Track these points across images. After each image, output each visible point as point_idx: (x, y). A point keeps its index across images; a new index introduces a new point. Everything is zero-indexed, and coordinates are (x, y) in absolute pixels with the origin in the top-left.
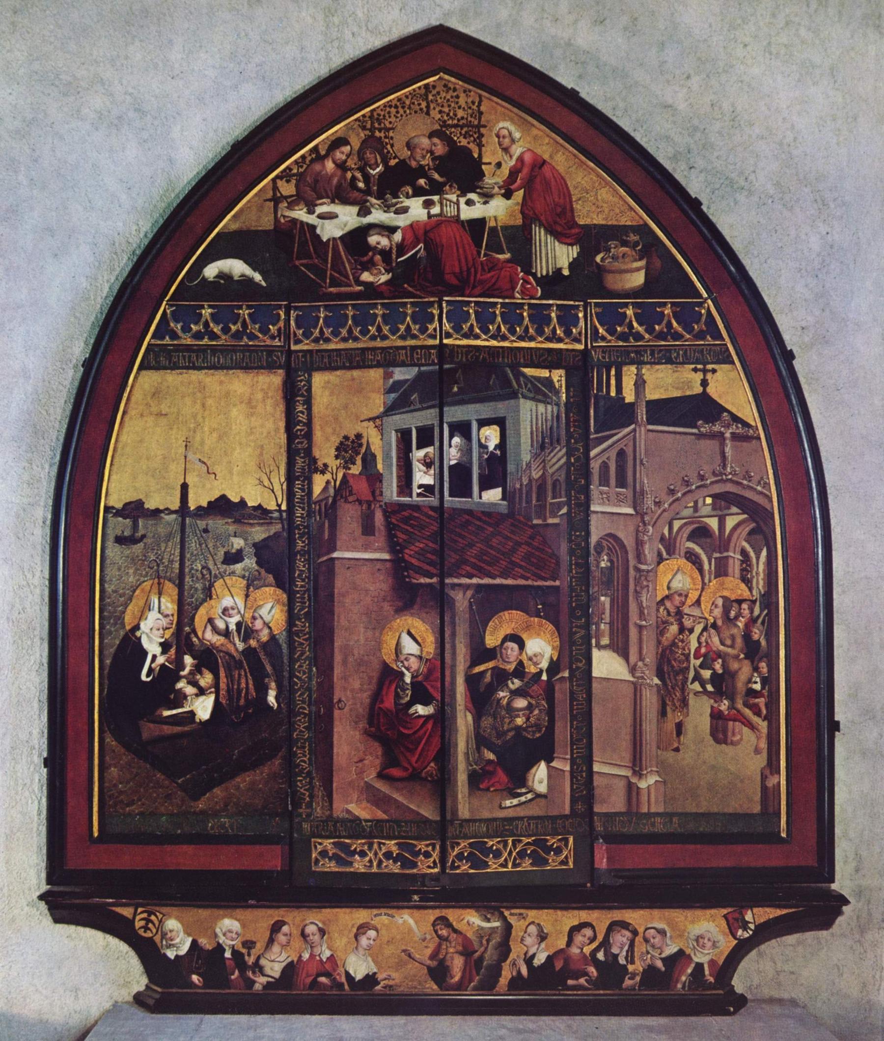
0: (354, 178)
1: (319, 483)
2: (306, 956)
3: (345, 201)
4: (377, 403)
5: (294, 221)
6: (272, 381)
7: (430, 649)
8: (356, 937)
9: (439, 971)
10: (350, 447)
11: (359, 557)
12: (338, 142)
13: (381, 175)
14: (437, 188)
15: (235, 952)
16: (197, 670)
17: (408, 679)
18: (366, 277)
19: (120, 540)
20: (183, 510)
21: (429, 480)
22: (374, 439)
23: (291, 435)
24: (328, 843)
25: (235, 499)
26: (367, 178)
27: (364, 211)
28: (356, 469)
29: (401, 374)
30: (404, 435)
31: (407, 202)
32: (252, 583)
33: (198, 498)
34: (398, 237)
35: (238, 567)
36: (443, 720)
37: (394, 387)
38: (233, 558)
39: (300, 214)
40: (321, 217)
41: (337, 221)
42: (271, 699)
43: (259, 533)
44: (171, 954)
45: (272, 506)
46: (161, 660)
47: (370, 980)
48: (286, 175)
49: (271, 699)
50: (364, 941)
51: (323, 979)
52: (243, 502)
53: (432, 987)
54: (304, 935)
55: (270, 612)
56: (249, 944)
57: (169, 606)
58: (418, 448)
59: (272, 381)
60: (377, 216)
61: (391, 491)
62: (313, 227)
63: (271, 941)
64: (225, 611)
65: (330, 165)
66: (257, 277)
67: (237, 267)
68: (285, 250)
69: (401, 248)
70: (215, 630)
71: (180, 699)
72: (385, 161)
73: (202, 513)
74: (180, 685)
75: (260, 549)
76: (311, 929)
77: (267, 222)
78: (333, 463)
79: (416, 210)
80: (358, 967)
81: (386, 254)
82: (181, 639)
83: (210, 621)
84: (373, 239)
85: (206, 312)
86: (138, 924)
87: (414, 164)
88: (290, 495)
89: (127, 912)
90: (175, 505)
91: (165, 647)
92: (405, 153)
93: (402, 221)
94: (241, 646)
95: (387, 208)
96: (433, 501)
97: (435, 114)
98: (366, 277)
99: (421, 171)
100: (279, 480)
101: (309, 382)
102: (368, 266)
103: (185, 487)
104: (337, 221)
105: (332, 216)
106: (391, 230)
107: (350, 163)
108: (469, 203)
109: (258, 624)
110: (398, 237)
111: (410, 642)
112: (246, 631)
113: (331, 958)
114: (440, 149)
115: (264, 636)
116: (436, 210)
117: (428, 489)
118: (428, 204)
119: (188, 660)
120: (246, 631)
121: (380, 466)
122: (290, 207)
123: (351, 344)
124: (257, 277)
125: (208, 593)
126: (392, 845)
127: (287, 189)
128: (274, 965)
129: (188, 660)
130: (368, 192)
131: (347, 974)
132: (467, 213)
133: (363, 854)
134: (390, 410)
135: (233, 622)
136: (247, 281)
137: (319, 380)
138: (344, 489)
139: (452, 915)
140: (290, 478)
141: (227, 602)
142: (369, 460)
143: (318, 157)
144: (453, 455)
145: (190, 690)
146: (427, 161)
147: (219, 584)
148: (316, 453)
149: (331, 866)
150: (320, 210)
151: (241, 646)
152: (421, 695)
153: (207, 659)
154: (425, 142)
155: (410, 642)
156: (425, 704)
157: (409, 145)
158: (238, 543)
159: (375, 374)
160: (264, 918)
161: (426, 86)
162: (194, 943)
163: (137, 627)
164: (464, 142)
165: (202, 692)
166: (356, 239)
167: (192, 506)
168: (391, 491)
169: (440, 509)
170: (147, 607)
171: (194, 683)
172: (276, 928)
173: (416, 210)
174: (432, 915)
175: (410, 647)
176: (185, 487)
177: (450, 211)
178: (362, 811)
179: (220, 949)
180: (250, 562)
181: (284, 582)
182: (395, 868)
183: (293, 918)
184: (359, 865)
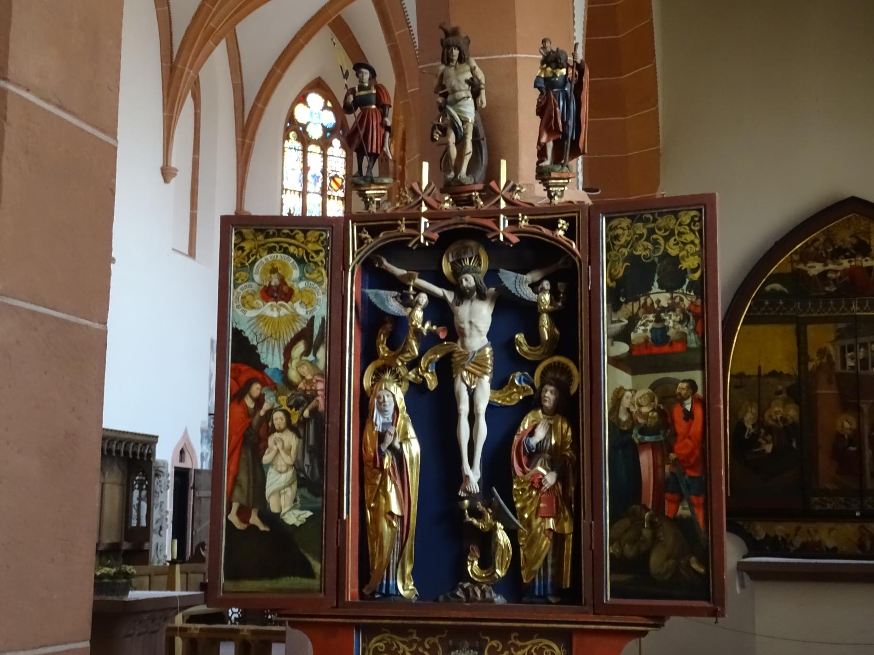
0: (821, 254)
1: (810, 365)
2: (810, 540)
3: (819, 261)
4: (832, 337)
5: (799, 269)
6: (791, 328)
7: (855, 426)
8: (829, 533)
9: (861, 546)
10: (822, 352)
11: (826, 391)
12: (815, 240)
13: (832, 252)
14: (853, 256)
15: (783, 539)
16: (766, 434)
17: (846, 436)
18: (827, 289)
19: (737, 387)
20: (759, 375)
21: (852, 364)
22: (831, 349)
23: (799, 348)
24: (817, 499)
25: (778, 370)
26: (826, 253)
27: (826, 265)
28: (825, 360)
29: (841, 325)
30: (843, 349)
31: (842, 261)
32: (785, 402)
33: (765, 371)
34: (839, 274)
35: (780, 396)
36: (860, 453)
37: (839, 330)
38: (780, 393)
39: (801, 266)
40: (810, 267)
41: (815, 269)
42: (794, 445)
43: (788, 384)
44: (758, 538)
45: (792, 373)
46: (752, 430)
47: (835, 549)
48: (796, 252)
49: (794, 445)
50: (832, 534)
51: (817, 549)
52: (781, 373)
53: (859, 552)
54: (808, 532)
55: (792, 412)
56: (788, 535)
57: (755, 410)
58: (849, 351)
59: (791, 328)
60: (831, 266)
61: (838, 368)
62: (806, 272)
63: (796, 534)
64: (776, 413)
65: (812, 249)
66: (786, 290)
67: (777, 286)
68: (796, 279)
69: (840, 278)
70: (773, 420)
71: (759, 445)
72: (833, 247)
73: (766, 376)
74: (760, 440)
75: (789, 390)
76: (811, 530)
77: (788, 269)
78: (816, 358)
79: (846, 264)
80: (830, 544)
81: (834, 280)
82: (759, 423)
83: (770, 416)
84: (830, 275)
85: (767, 303)
86: (746, 527)
87: (844, 247)
88: (799, 370)
89: (741, 523)
90: (756, 373)
91: (754, 425)
92: (841, 244)
93: (840, 268)
94: (782, 425)
95: (834, 263)
96: (853, 371)
97: (852, 229)
98: (827, 289)
99: (847, 250)
100: (795, 365)
101: (806, 328)
102: (828, 285)
103: (760, 368)
104: (815, 269)
105: (814, 267)
106: (836, 271)
107: (821, 247)
108: (866, 261)
109: (788, 418)
110: (839, 274)
111: (847, 424)
112: (784, 419)
113: (820, 541)
114: (854, 241)
115: (791, 421)
116: (853, 264)
117: (852, 367)
118: (850, 262)
119: (762, 431)
120: (784, 419)
121: (834, 359)
122: (798, 264)
123: (821, 315)
124: (786, 290)
125: (769, 406)
126: (842, 499)
127: (796, 258)
128: (798, 542)
129: (762, 431)
130: (827, 258)
131: (826, 547)
132: (866, 264)
133: (830, 503)
134: (837, 338)
135: (779, 416)
136: (781, 292)
137: (810, 328)
138: (819, 368)
139: (866, 525)
140: (799, 363)
141: (777, 409)
142: (829, 357)
143: (807, 245)
144: (861, 354)
145: (763, 442)
146: (849, 246)
147: (773, 403)
148: (809, 354)
149: (818, 508)
150: (809, 265)
151: (782, 425)
152: (851, 442)
153: (769, 430)
154: (848, 239)
155: (847, 424)
156: (853, 446)
157: (843, 241)
158: (780, 387)
159: (831, 326)
160: (793, 525)
161: (848, 219)
162: (767, 535)
163: (743, 419)
164: (863, 238)
165: (768, 442)
166: (823, 275)
167: (763, 373)
168: (838, 368)
169: (857, 375)
170: (746, 412)
171: (765, 439)
172: (798, 529)
173: (846, 264)
174: (857, 525)
175: (847, 425)
176: (760, 368)
177: (859, 263)
178: (830, 486)
179: (776, 537)
180: (784, 395)
181: (797, 402)
182: (844, 508)
183: (804, 526)
184: (829, 507)
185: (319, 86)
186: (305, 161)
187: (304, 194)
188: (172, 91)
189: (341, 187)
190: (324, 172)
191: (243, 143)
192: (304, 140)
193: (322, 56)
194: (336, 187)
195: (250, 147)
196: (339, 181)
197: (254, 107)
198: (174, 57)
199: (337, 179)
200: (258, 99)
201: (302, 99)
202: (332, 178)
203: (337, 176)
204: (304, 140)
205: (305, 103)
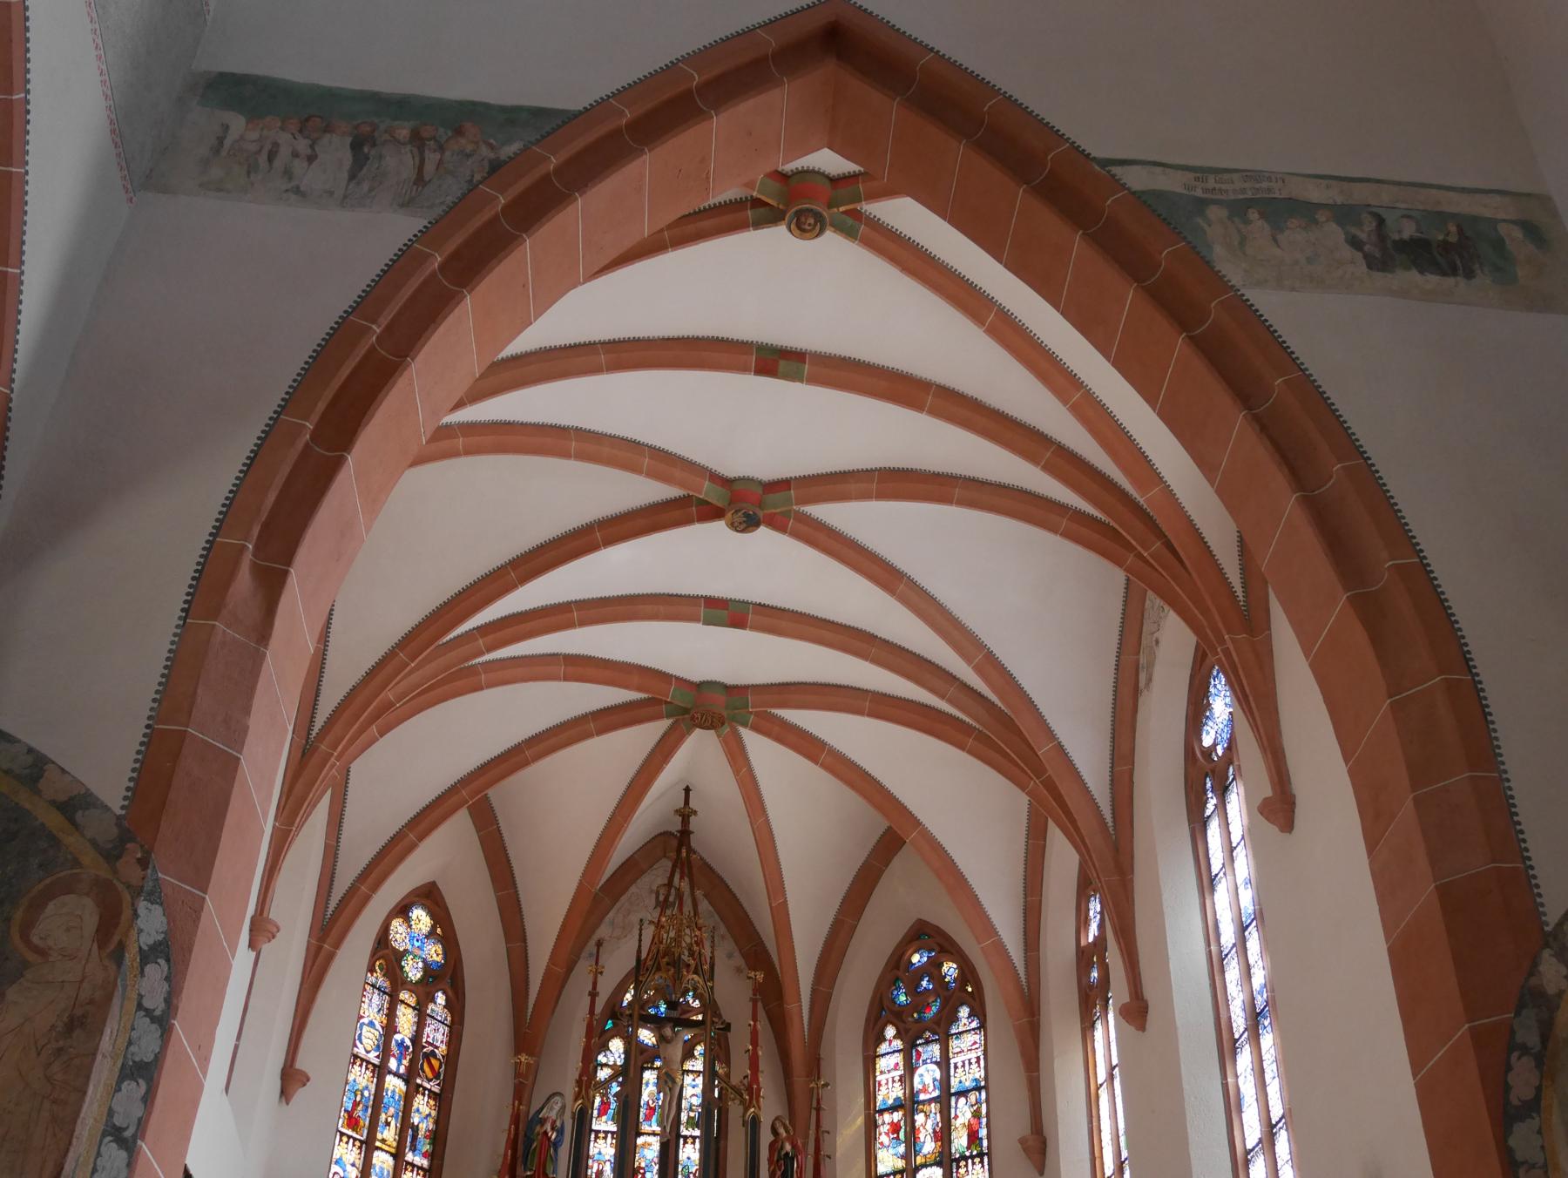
185: (429, 896)
186: (391, 1015)
187: (380, 1071)
188: (299, 787)
189: (437, 1076)
190: (416, 1039)
191: (320, 948)
192: (396, 979)
193: (447, 854)
194: (430, 1075)
195: (330, 957)
196: (435, 1063)
197: (352, 891)
198: (314, 734)
199: (433, 1061)
200: (363, 876)
201: (403, 911)
202: (427, 1056)
203: (433, 1054)
204: (396, 979)
205: (407, 920)
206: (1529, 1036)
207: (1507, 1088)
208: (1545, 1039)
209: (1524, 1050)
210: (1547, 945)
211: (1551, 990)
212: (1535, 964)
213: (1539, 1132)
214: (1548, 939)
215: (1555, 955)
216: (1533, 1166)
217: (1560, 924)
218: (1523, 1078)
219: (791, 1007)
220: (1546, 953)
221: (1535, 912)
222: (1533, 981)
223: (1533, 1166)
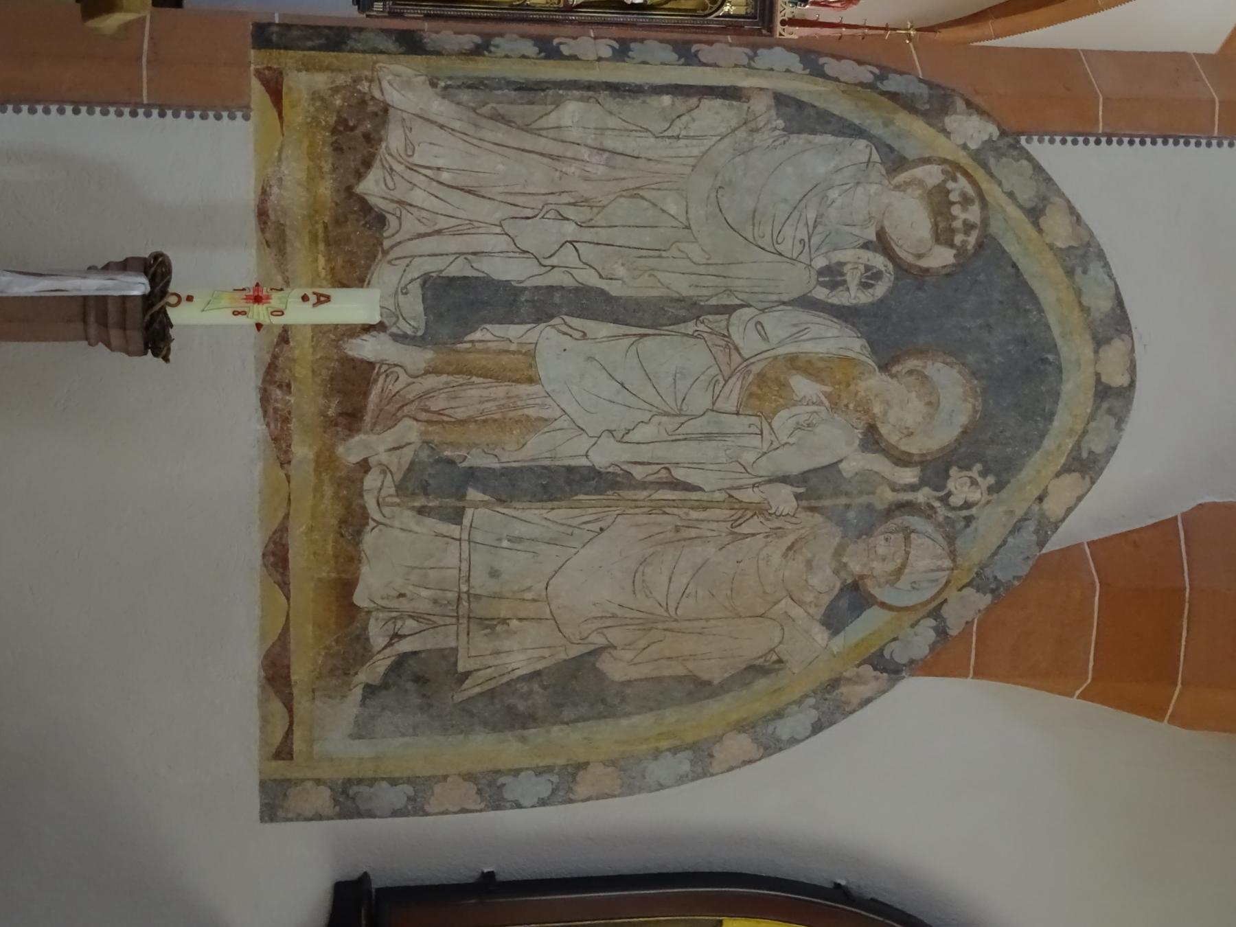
206: (894, 84)
207: (839, 58)
208: (893, 96)
209: (881, 78)
210: (1003, 133)
211: (951, 122)
212: (981, 112)
213: (788, 71)
214: (1010, 140)
215: (990, 140)
216: (751, 58)
217: (1030, 158)
218: (847, 70)
219: (990, 26)
220: (993, 130)
221: (1045, 132)
222: (960, 104)
223: (751, 58)
